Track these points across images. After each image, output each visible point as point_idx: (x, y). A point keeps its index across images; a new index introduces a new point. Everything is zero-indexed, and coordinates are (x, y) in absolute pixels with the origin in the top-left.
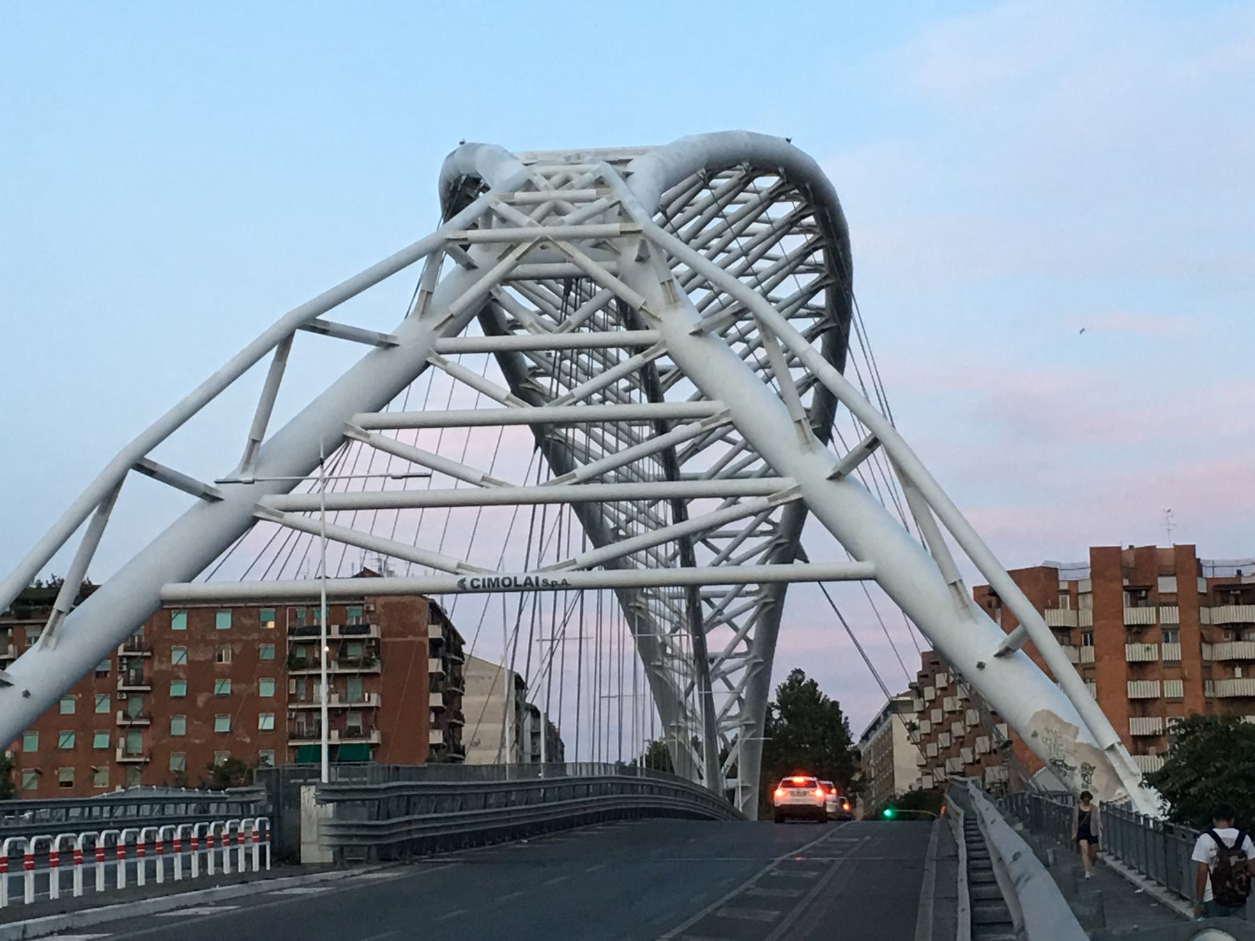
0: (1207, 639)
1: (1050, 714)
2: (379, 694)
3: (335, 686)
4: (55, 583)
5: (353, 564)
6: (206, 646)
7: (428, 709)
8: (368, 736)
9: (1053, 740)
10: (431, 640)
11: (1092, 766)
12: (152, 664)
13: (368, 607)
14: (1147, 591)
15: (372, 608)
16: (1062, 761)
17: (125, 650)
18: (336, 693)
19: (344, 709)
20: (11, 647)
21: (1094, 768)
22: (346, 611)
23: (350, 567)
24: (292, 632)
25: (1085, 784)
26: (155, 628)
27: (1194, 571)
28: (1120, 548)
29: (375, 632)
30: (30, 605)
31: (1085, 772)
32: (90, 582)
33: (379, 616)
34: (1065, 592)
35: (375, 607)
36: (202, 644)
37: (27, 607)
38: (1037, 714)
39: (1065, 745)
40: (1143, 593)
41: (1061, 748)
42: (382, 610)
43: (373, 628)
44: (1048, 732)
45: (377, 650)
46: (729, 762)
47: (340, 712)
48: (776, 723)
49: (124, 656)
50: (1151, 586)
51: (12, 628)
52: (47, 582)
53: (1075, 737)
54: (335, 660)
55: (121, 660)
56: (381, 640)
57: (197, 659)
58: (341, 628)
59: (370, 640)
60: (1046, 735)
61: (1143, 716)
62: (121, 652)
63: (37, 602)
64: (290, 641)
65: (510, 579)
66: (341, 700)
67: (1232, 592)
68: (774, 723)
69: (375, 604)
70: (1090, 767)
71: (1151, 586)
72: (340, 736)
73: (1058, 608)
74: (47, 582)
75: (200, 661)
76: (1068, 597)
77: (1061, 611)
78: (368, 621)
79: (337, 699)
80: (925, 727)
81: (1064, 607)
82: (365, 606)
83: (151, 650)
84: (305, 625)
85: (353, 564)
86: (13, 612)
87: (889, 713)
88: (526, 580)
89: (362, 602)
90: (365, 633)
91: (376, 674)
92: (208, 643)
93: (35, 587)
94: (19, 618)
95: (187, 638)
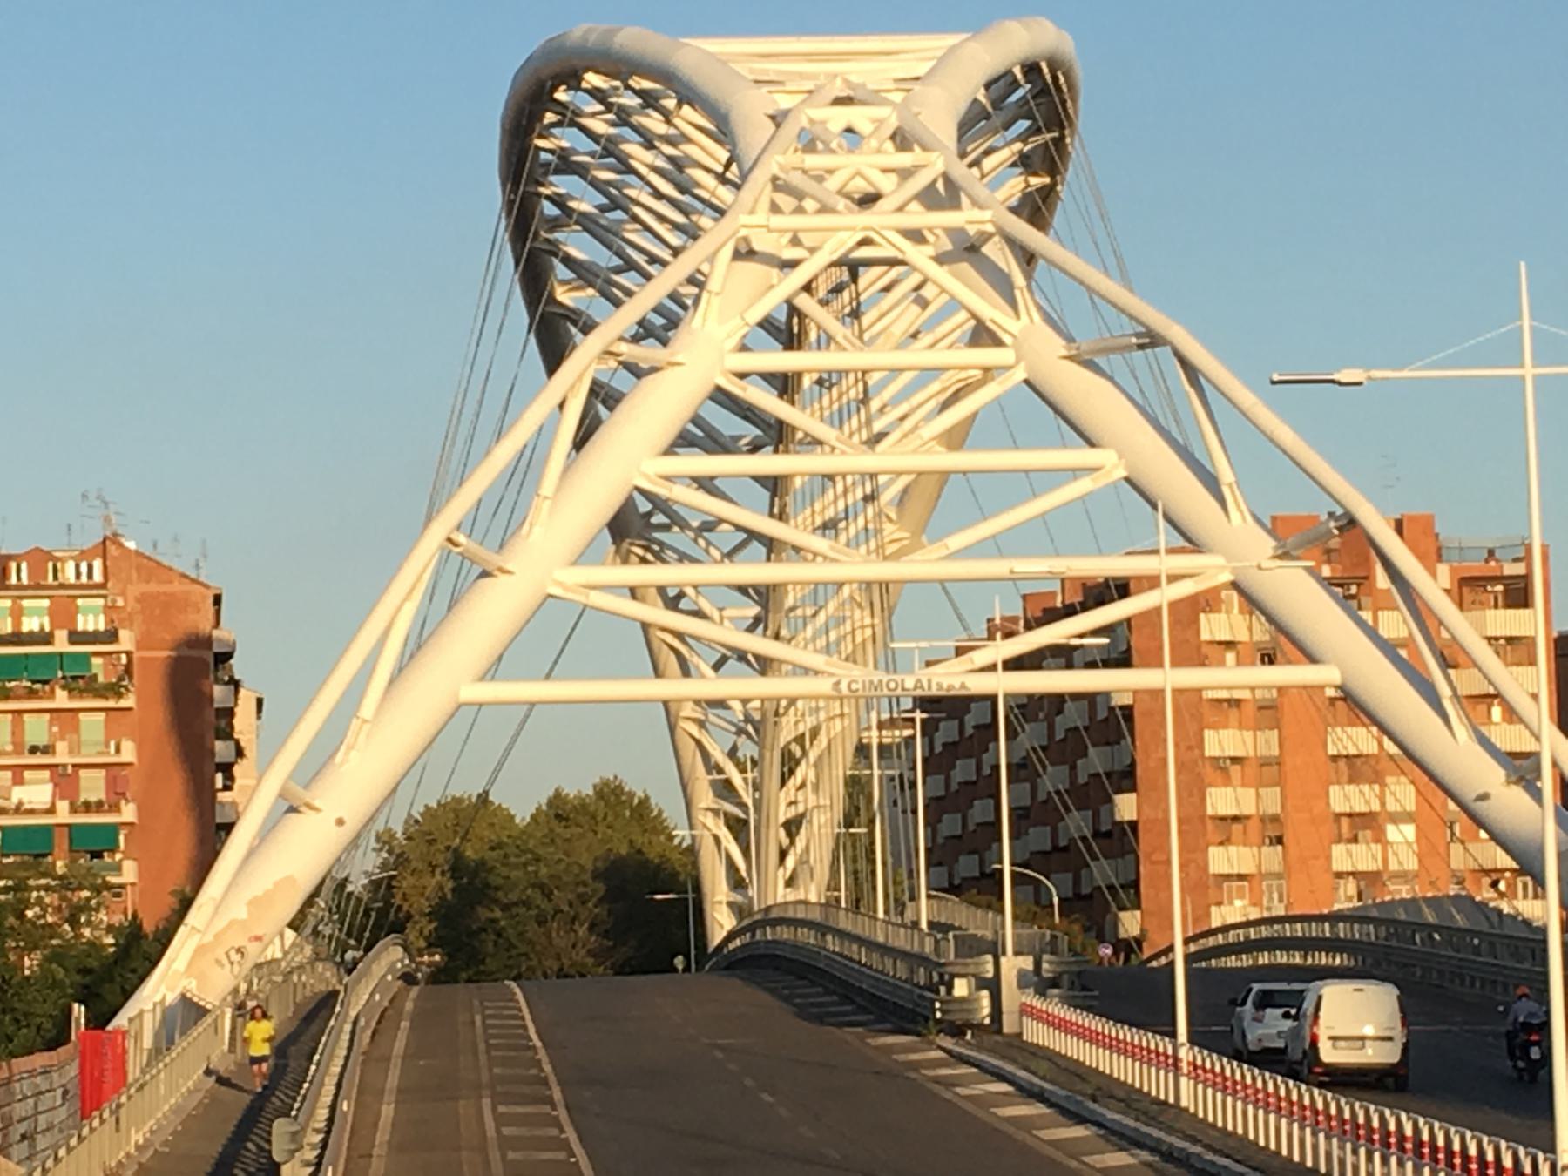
0: (1452, 663)
2: (133, 740)
3: (60, 729)
5: (69, 527)
7: (214, 767)
8: (114, 808)
10: (217, 655)
13: (114, 601)
14: (1359, 585)
15: (120, 602)
18: (63, 739)
19: (74, 766)
22: (77, 607)
23: (66, 529)
27: (1434, 557)
28: (1317, 517)
29: (126, 640)
33: (130, 614)
35: (125, 600)
40: (1354, 590)
42: (138, 607)
43: (124, 634)
45: (128, 670)
46: (790, 862)
47: (70, 770)
50: (1366, 578)
54: (63, 687)
56: (135, 656)
59: (118, 653)
61: (1351, 781)
66: (71, 752)
67: (1489, 588)
69: (123, 594)
71: (1366, 578)
72: (74, 810)
73: (1219, 611)
77: (1223, 616)
79: (67, 750)
81: (1228, 612)
82: (109, 599)
85: (69, 527)
90: (111, 643)
91: (129, 709)
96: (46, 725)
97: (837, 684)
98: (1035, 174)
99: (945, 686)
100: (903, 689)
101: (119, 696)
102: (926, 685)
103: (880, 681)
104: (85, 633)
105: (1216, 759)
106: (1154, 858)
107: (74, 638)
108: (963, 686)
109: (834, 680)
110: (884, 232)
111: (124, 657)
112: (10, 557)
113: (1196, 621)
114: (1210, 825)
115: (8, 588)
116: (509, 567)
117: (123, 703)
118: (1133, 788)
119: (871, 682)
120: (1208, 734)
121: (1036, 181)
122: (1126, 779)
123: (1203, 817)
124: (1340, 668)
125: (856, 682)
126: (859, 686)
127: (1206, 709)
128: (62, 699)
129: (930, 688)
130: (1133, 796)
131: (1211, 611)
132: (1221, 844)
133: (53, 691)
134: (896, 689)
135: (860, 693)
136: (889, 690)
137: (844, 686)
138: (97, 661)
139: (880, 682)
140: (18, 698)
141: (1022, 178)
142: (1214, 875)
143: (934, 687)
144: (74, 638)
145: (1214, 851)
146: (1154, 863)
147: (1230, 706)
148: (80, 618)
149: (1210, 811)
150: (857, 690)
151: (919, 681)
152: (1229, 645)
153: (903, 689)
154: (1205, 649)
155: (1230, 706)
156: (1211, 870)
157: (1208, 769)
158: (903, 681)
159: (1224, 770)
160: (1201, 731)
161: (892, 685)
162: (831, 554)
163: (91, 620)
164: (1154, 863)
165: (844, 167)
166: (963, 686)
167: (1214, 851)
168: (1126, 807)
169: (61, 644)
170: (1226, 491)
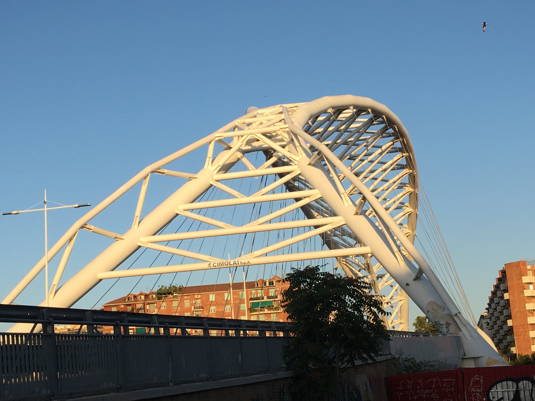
1: (433, 302)
3: (267, 318)
4: (170, 287)
6: (222, 306)
9: (435, 313)
11: (450, 323)
12: (204, 312)
13: (277, 289)
15: (278, 290)
16: (439, 322)
17: (194, 308)
20: (156, 310)
21: (451, 324)
22: (269, 291)
24: (251, 299)
25: (448, 331)
26: (204, 301)
30: (162, 295)
31: (447, 326)
32: (182, 286)
34: (529, 270)
35: (279, 289)
36: (220, 306)
37: (161, 296)
38: (428, 303)
39: (439, 315)
41: (438, 316)
43: (279, 296)
44: (433, 310)
48: (428, 324)
49: (194, 311)
51: (156, 303)
52: (168, 287)
53: (444, 312)
54: (266, 309)
55: (193, 312)
57: (219, 310)
58: (267, 297)
60: (432, 311)
62: (193, 309)
63: (164, 294)
64: (250, 303)
65: (228, 263)
68: (427, 324)
69: (279, 288)
70: (449, 324)
73: (527, 275)
74: (168, 287)
75: (220, 311)
76: (531, 272)
77: (528, 277)
78: (277, 294)
80: (491, 324)
81: (530, 275)
83: (203, 308)
84: (255, 297)
86: (156, 298)
87: (481, 319)
88: (234, 263)
89: (274, 287)
92: (222, 305)
93: (164, 288)
94: (158, 300)
95: (215, 303)
96: (264, 317)
97: (210, 264)
98: (405, 153)
99: (243, 263)
100: (230, 265)
101: (278, 310)
102: (237, 263)
103: (223, 263)
104: (271, 296)
105: (530, 310)
106: (517, 334)
107: (268, 298)
108: (249, 262)
109: (209, 263)
110: (256, 134)
111: (279, 301)
112: (255, 282)
113: (521, 278)
114: (529, 325)
115: (254, 288)
116: (123, 238)
117: (279, 311)
118: (511, 319)
119: (220, 263)
120: (526, 304)
121: (404, 154)
122: (509, 317)
123: (527, 324)
124: (371, 248)
125: (216, 263)
126: (217, 265)
127: (526, 299)
128: (266, 311)
129: (238, 264)
130: (511, 320)
131: (524, 276)
132: (533, 330)
133: (264, 310)
134: (228, 265)
135: (217, 267)
136: (226, 265)
137: (212, 265)
138: (273, 302)
139: (223, 263)
140: (258, 311)
141: (401, 154)
142: (531, 338)
143: (239, 263)
144: (268, 298)
145: (530, 332)
146: (517, 336)
147: (532, 298)
148: (270, 294)
149: (529, 323)
150: (216, 266)
151: (235, 261)
152: (530, 283)
153: (230, 265)
154: (524, 285)
155: (532, 298)
156: (530, 337)
157: (528, 313)
158: (230, 262)
159: (532, 313)
160: (525, 303)
161: (226, 264)
162: (224, 227)
163: (272, 292)
164: (517, 336)
165: (255, 122)
166: (249, 262)
167: (530, 332)
168: (510, 323)
169: (265, 299)
170: (342, 195)
